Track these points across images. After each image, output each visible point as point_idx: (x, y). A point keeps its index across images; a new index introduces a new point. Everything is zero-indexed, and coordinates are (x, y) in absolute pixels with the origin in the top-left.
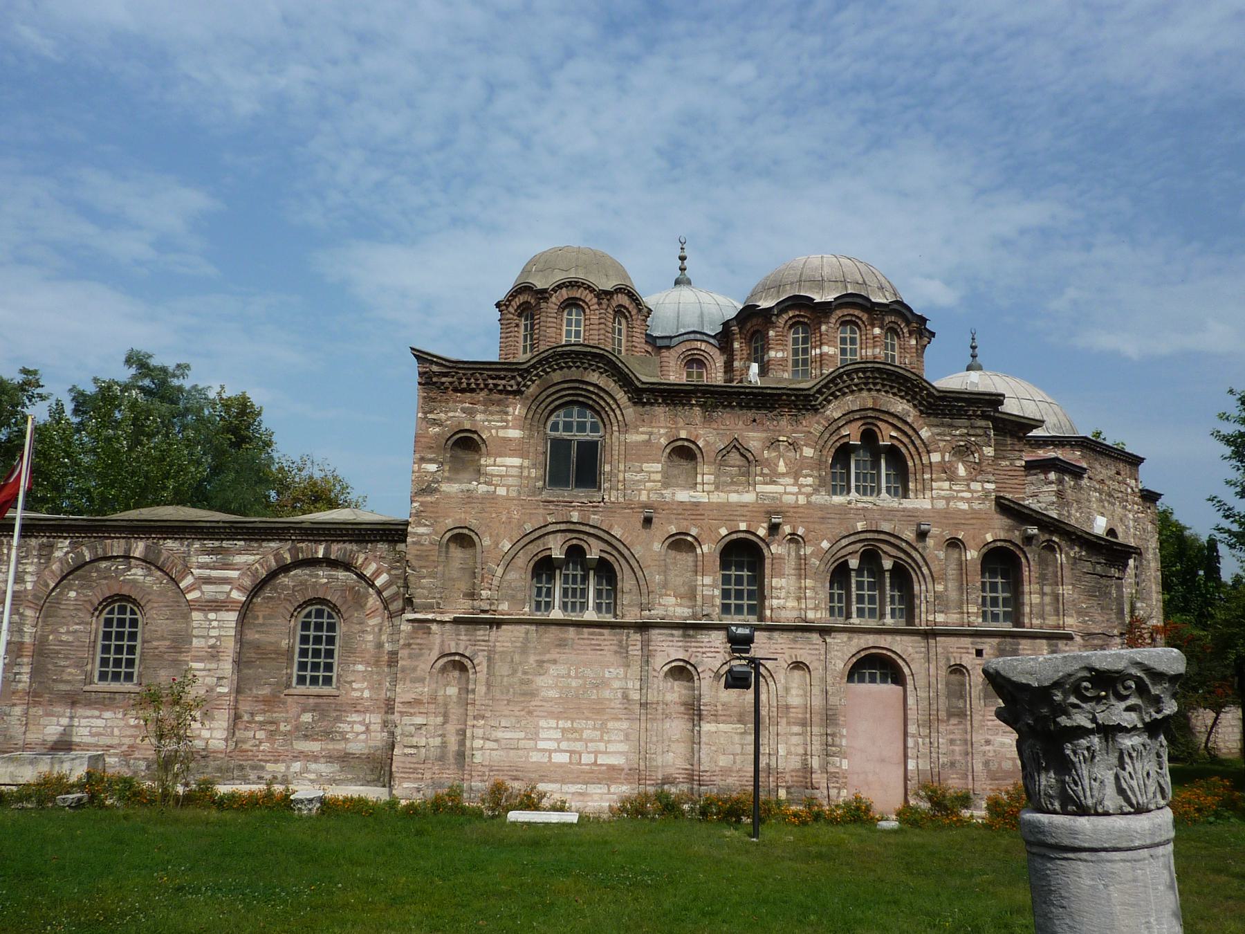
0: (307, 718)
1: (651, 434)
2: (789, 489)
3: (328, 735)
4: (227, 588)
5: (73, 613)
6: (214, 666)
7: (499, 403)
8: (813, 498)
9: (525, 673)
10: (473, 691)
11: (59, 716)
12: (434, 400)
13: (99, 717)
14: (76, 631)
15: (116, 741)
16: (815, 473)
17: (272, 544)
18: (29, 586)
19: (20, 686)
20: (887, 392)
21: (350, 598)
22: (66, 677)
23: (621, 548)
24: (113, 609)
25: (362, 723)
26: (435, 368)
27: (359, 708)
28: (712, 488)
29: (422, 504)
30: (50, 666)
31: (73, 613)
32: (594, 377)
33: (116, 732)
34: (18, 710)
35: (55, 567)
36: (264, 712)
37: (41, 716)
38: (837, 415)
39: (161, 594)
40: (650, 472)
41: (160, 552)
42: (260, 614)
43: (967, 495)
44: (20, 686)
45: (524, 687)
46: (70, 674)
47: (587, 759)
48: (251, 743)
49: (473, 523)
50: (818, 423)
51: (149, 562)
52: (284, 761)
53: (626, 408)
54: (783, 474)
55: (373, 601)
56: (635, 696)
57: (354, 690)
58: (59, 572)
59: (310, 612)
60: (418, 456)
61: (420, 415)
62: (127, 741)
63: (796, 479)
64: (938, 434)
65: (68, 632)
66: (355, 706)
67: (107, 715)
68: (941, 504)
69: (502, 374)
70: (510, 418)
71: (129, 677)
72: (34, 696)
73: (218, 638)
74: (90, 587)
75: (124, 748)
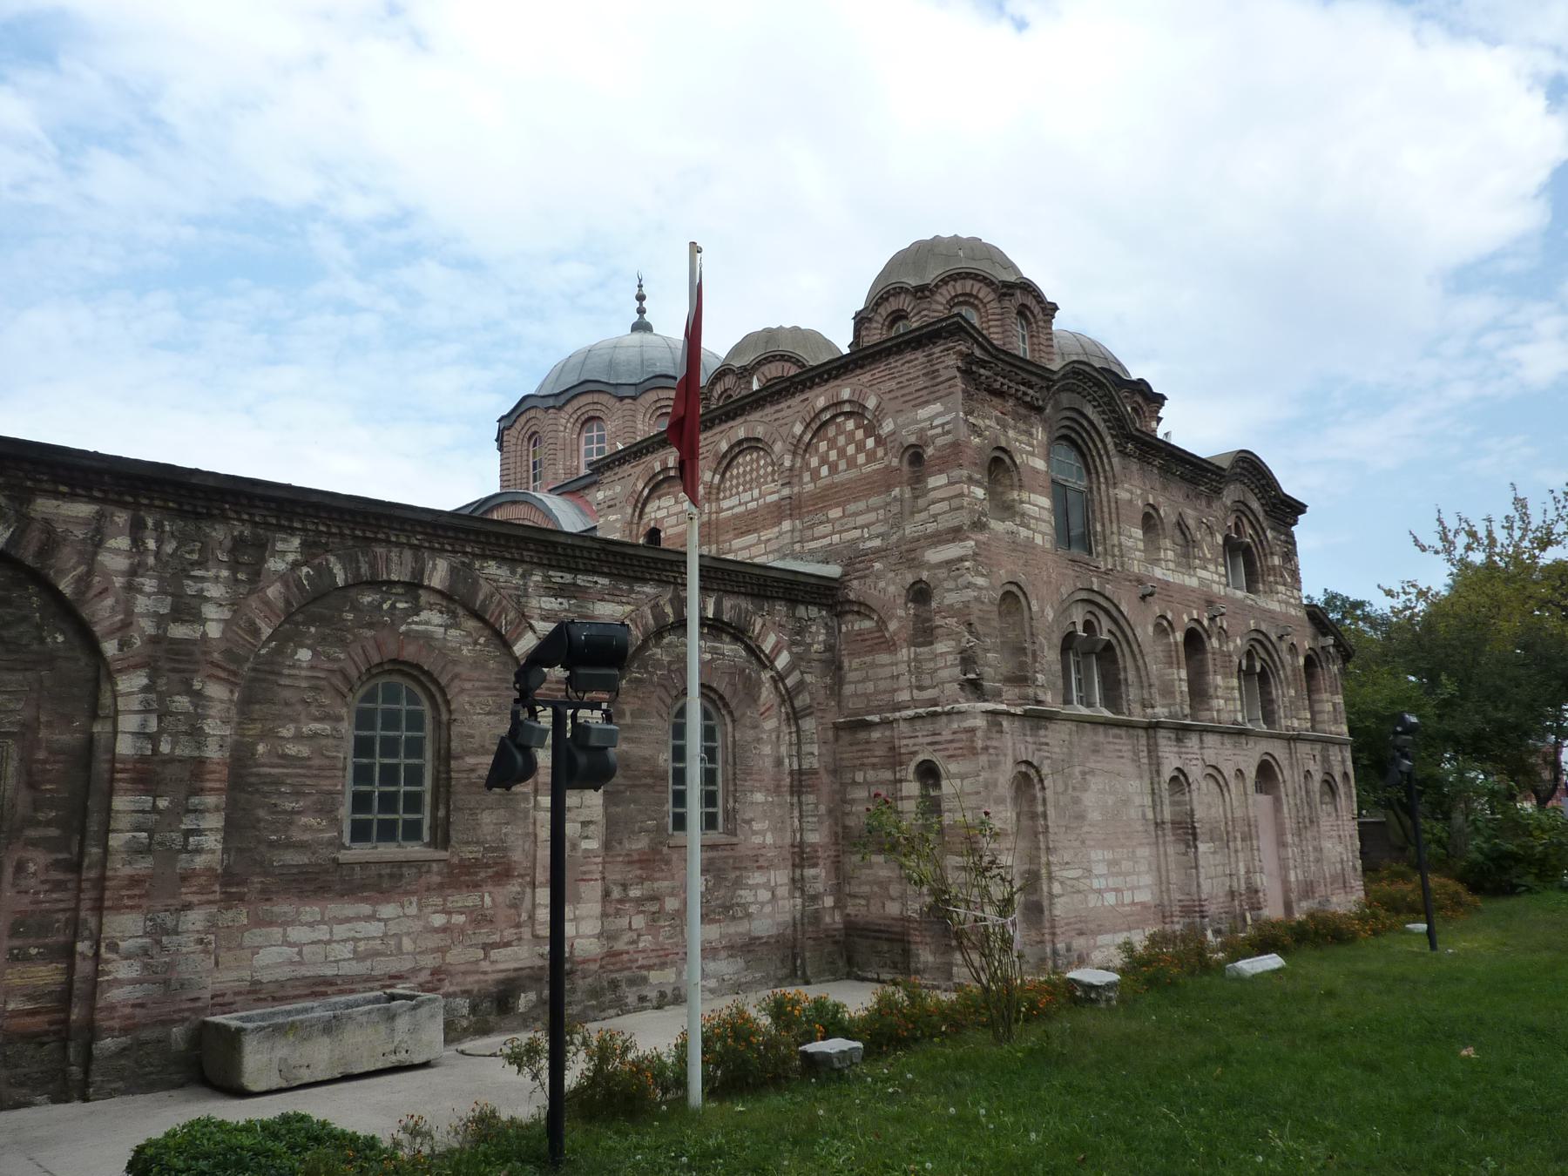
5: (309, 696)
7: (1025, 419)
9: (1074, 789)
10: (1045, 816)
11: (285, 924)
13: (371, 918)
14: (315, 735)
15: (406, 965)
17: (647, 589)
18: (214, 631)
19: (200, 862)
21: (740, 686)
22: (297, 836)
24: (374, 689)
25: (766, 886)
26: (978, 352)
27: (762, 862)
29: (977, 542)
30: (261, 813)
31: (309, 696)
32: (1089, 411)
33: (407, 944)
34: (195, 920)
35: (273, 591)
36: (641, 880)
37: (245, 928)
39: (476, 664)
41: (476, 582)
42: (627, 709)
44: (200, 862)
46: (306, 828)
47: (1127, 899)
48: (626, 937)
51: (457, 600)
52: (673, 964)
55: (767, 694)
56: (1150, 815)
58: (281, 604)
62: (429, 961)
65: (299, 737)
67: (388, 910)
69: (1034, 379)
71: (413, 832)
72: (231, 884)
74: (342, 643)
75: (424, 976)
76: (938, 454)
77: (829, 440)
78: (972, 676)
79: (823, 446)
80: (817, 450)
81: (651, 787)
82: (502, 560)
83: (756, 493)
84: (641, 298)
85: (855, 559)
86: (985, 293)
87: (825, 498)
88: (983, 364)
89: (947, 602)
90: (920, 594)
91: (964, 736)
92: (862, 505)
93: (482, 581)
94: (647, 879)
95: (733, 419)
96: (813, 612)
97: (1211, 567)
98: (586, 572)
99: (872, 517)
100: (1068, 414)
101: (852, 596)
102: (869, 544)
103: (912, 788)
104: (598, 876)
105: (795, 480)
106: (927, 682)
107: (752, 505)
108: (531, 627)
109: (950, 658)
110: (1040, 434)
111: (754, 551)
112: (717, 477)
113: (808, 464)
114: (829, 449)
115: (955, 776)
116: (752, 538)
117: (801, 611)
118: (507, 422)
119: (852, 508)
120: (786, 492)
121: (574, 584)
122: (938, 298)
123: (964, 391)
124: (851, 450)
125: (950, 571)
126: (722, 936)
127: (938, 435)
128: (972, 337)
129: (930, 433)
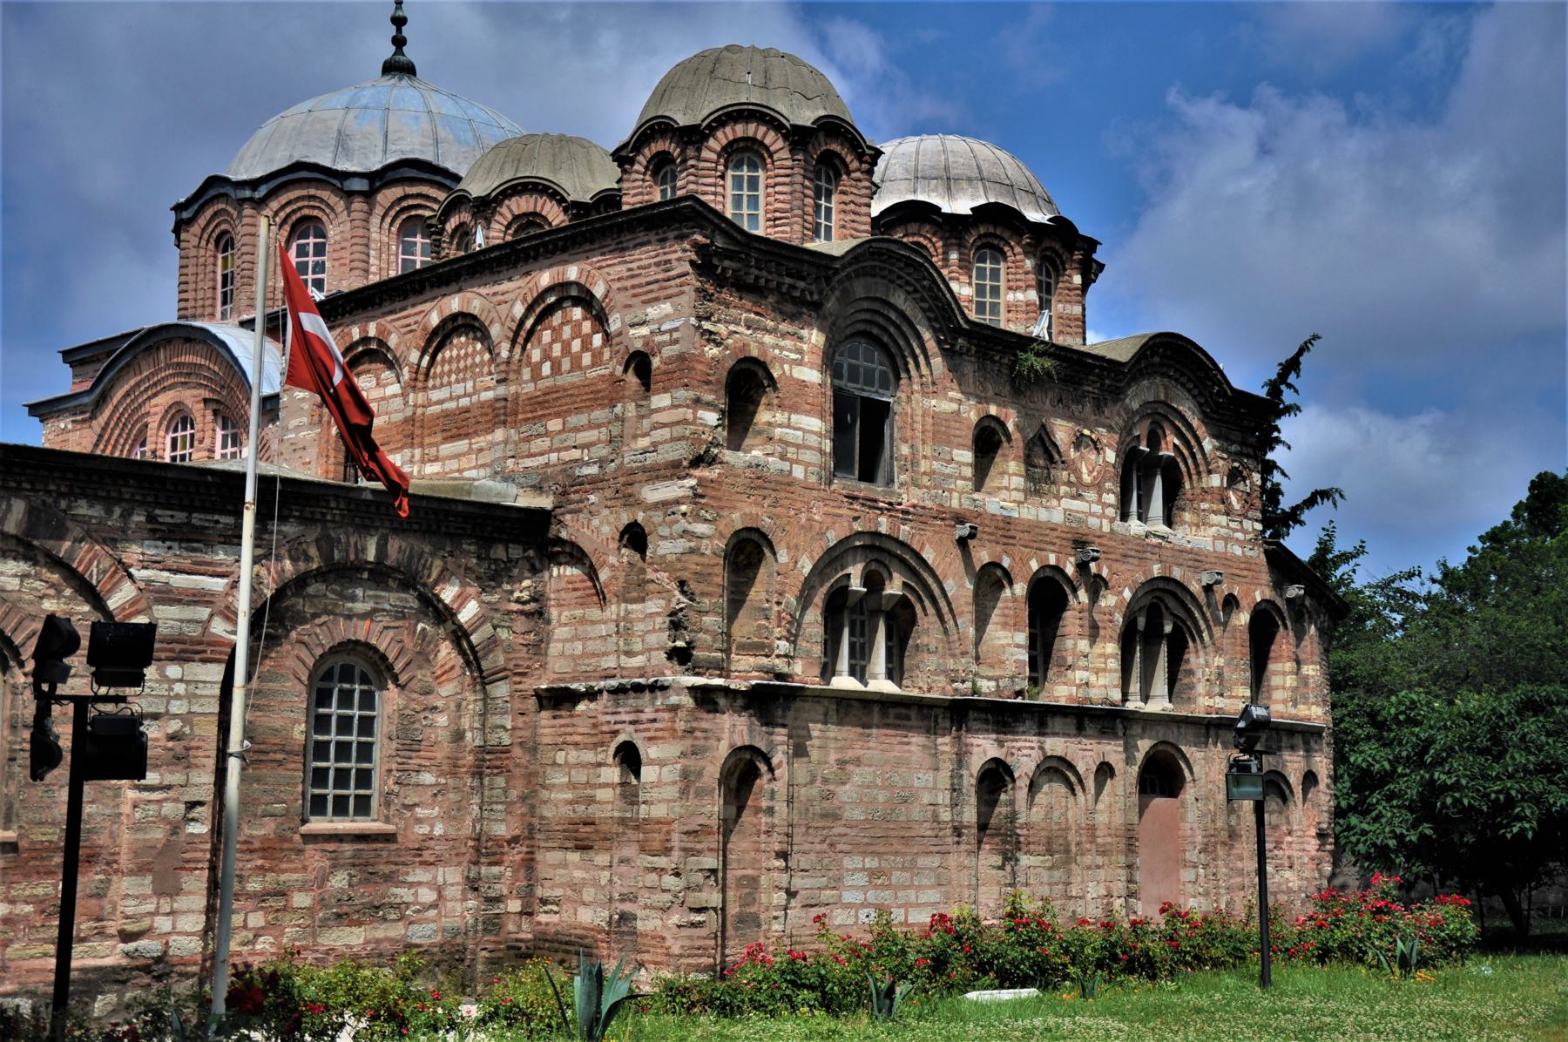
0: (339, 881)
3: (375, 911)
4: (203, 612)
6: (176, 778)
12: (708, 297)
23: (930, 581)
27: (427, 855)
32: (899, 299)
43: (1240, 535)
45: (826, 804)
49: (766, 523)
50: (1119, 414)
57: (419, 821)
59: (331, 670)
61: (693, 321)
66: (420, 853)
68: (1220, 546)
70: (805, 347)
73: (187, 718)
76: (663, 367)
77: (554, 329)
78: (680, 644)
79: (547, 336)
80: (540, 341)
81: (280, 763)
82: (93, 499)
83: (470, 385)
84: (399, 22)
85: (570, 486)
86: (772, 140)
87: (545, 404)
88: (725, 254)
89: (660, 552)
90: (635, 537)
91: (666, 715)
92: (582, 419)
93: (69, 524)
94: (271, 870)
95: (447, 284)
96: (516, 552)
97: (1091, 495)
98: (204, 510)
99: (591, 435)
100: (865, 305)
101: (564, 535)
102: (587, 471)
103: (613, 774)
104: (206, 865)
105: (512, 376)
106: (638, 647)
107: (465, 402)
108: (130, 576)
109: (659, 620)
110: (815, 338)
111: (464, 463)
112: (427, 358)
113: (529, 357)
114: (554, 341)
115: (652, 762)
116: (462, 445)
117: (499, 552)
118: (185, 214)
119: (573, 420)
120: (501, 390)
121: (189, 524)
122: (712, 143)
123: (697, 290)
124: (576, 345)
125: (666, 515)
126: (367, 942)
127: (664, 344)
128: (711, 222)
129: (658, 338)
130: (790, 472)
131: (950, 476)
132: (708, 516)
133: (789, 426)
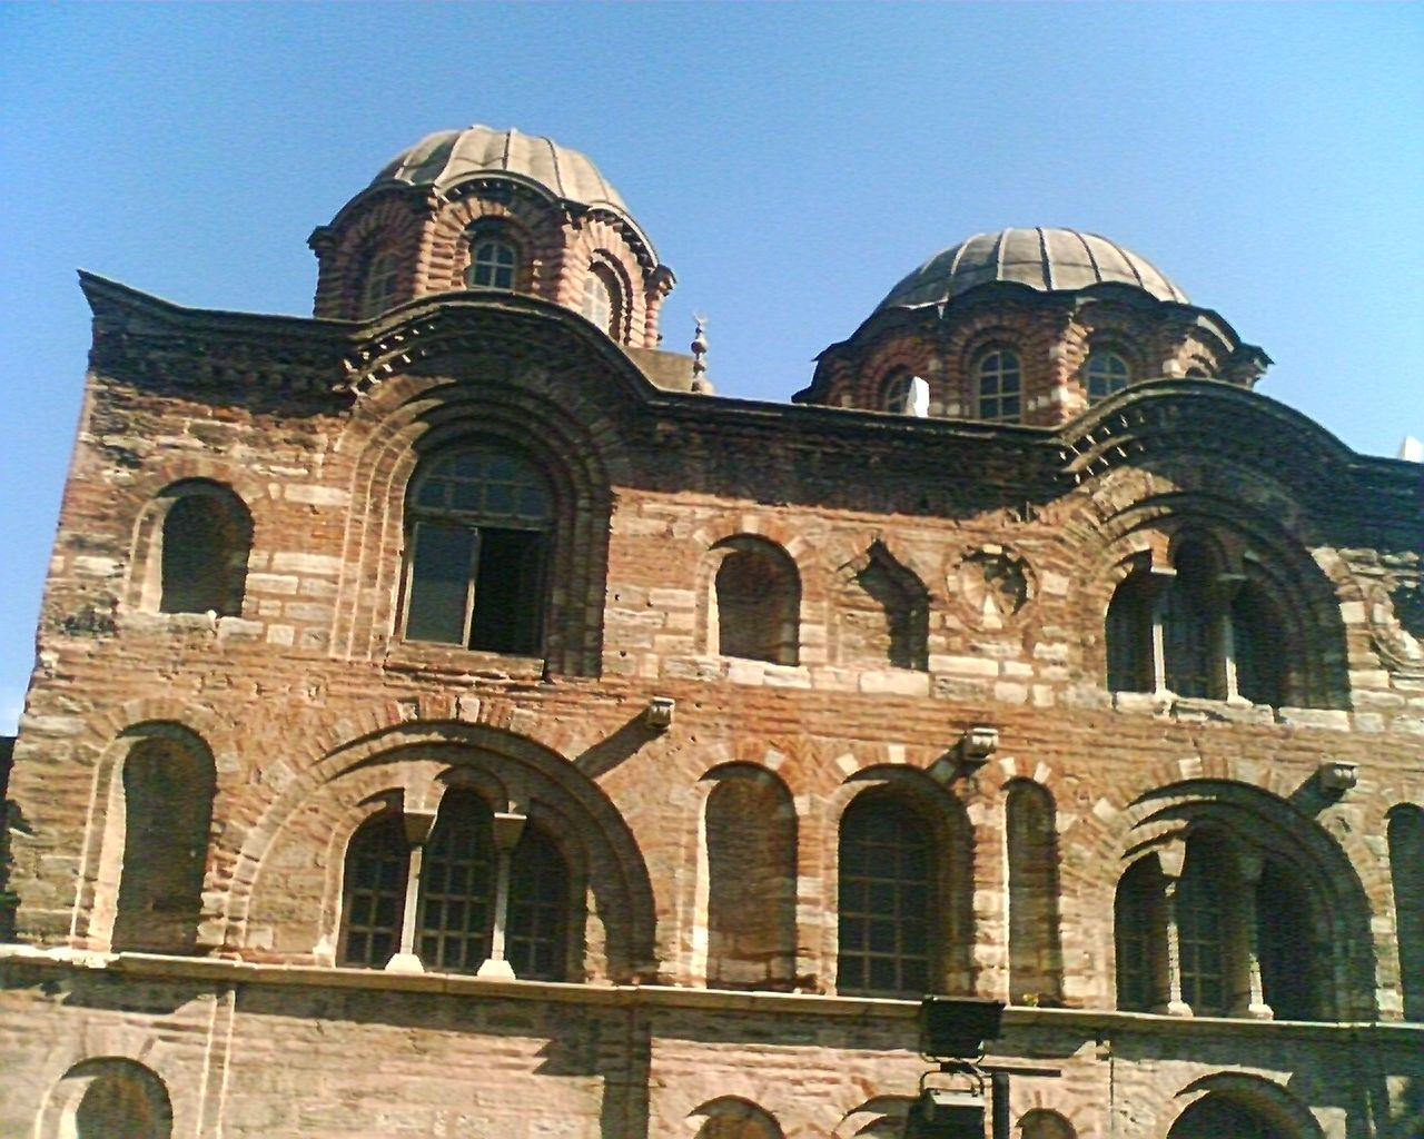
1: (675, 519)
2: (1014, 668)
8: (1071, 694)
16: (1075, 638)
20: (1234, 457)
26: (135, 325)
28: (822, 655)
32: (537, 379)
38: (1122, 501)
40: (666, 610)
53: (613, 455)
54: (994, 633)
60: (66, 534)
61: (84, 436)
63: (1028, 644)
64: (1357, 560)
130: (262, 637)
131: (642, 629)
132: (73, 706)
133: (268, 570)
